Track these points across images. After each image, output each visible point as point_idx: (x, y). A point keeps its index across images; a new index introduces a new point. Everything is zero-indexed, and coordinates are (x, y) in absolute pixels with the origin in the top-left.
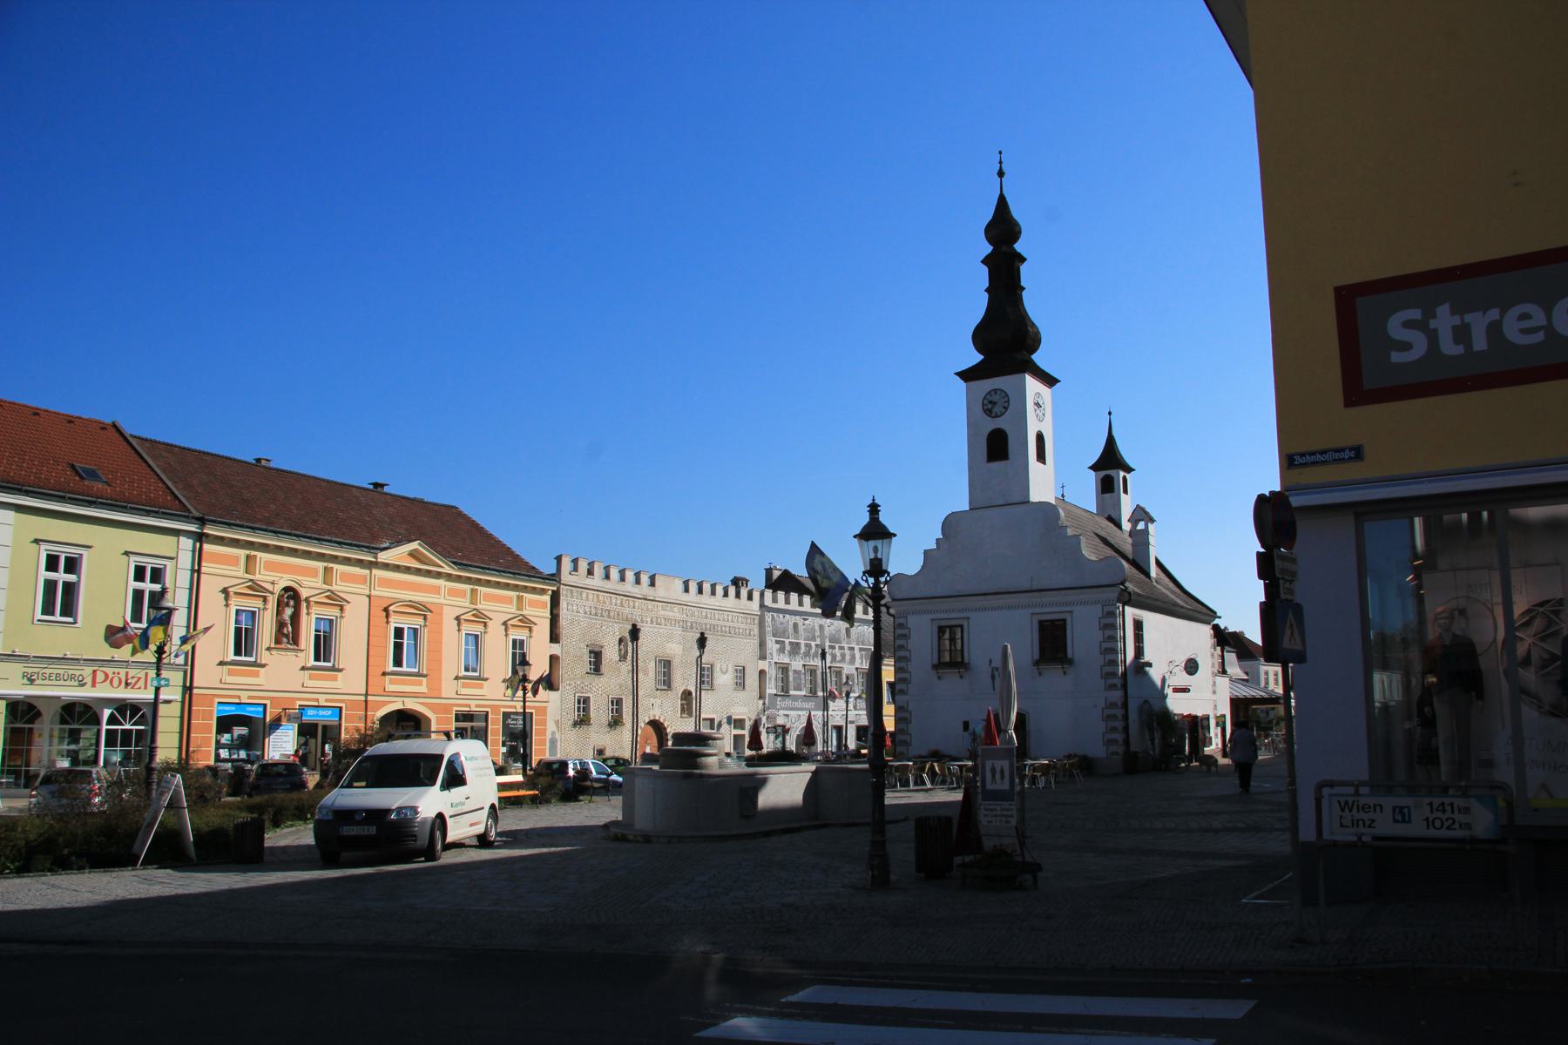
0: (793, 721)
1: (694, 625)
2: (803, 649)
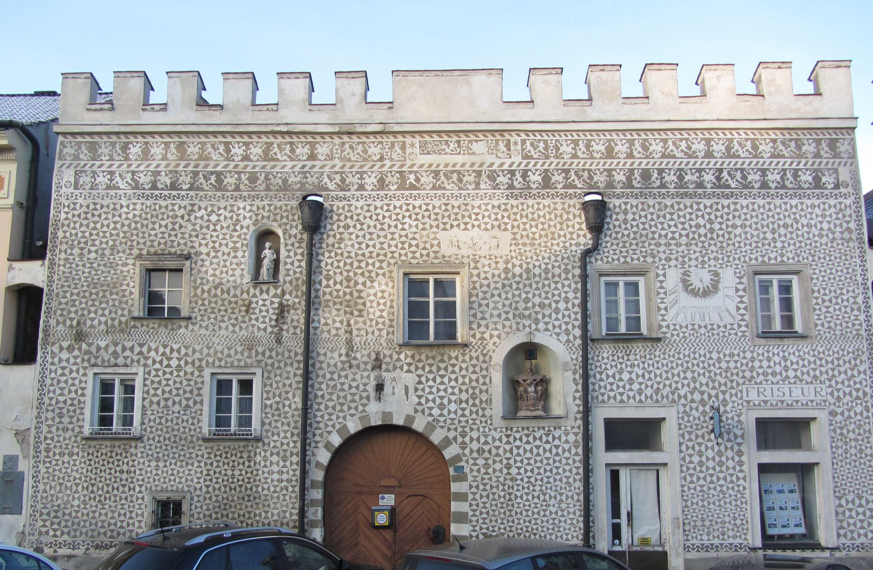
1: (557, 178)
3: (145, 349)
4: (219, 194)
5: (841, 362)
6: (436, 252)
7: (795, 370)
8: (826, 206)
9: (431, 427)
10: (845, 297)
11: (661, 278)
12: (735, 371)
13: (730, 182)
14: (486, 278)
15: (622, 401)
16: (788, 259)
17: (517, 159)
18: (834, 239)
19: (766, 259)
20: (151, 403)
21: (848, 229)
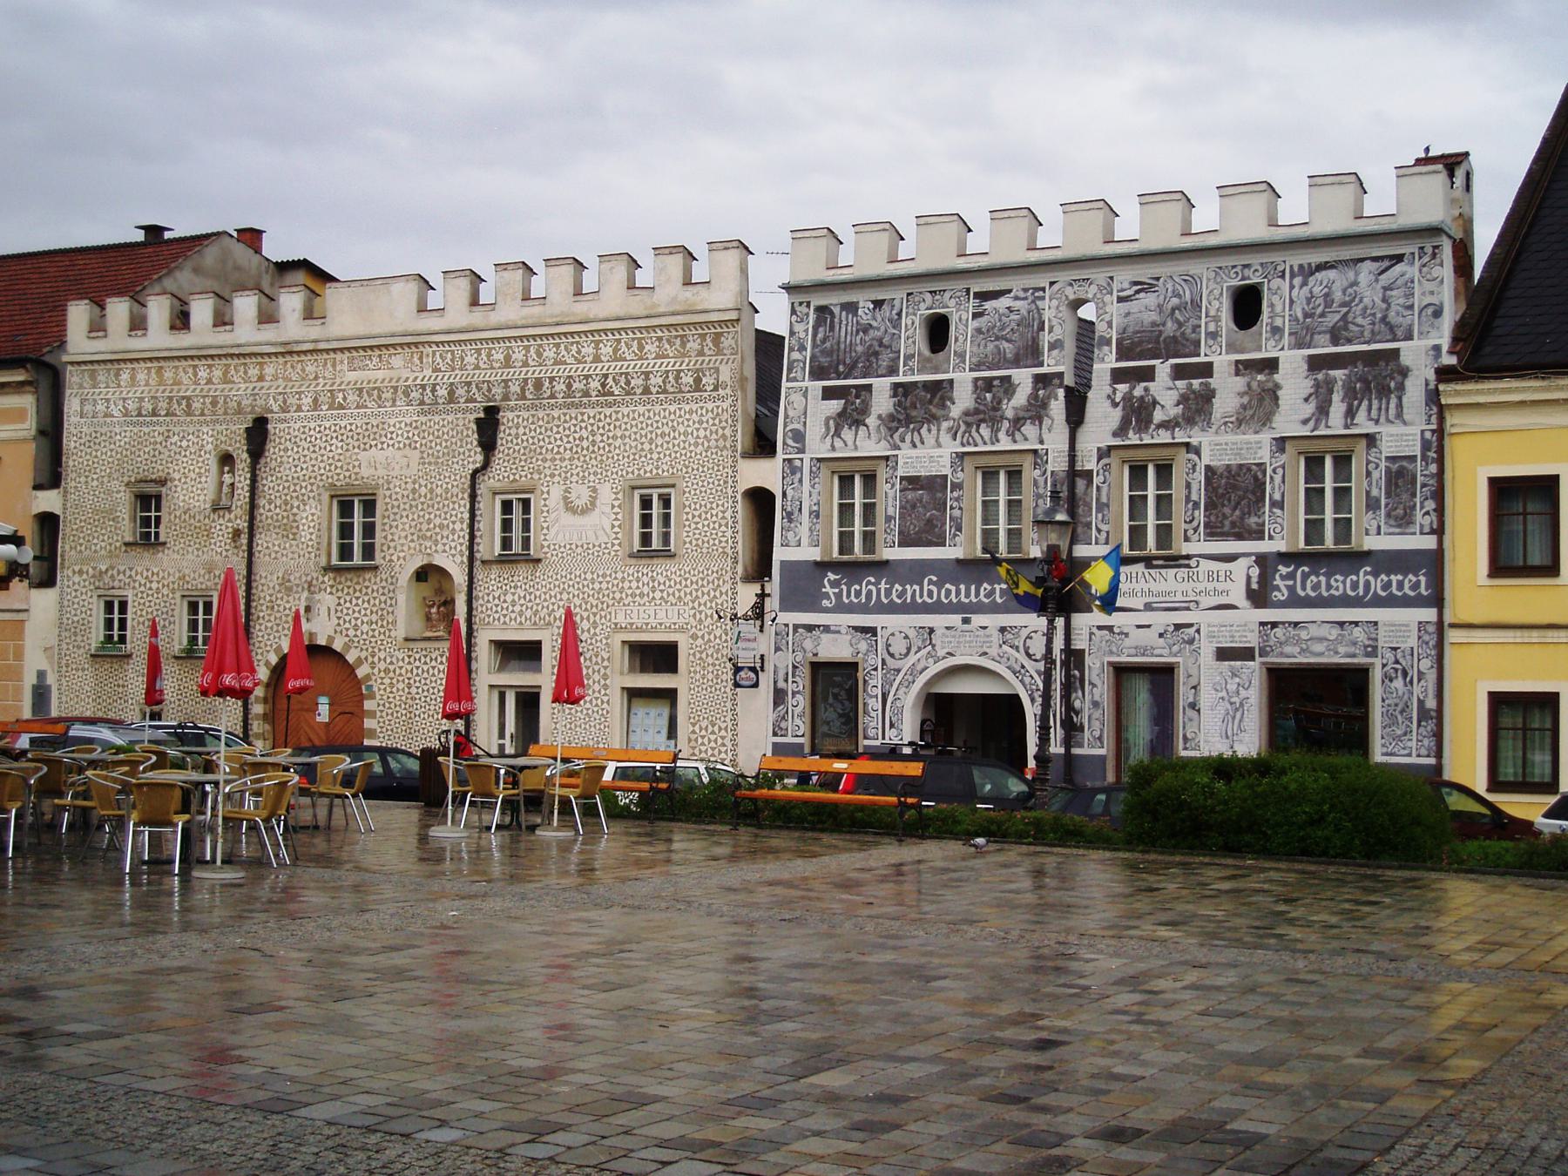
1: (461, 392)
2: (963, 399)
3: (133, 573)
4: (189, 419)
5: (705, 583)
6: (356, 474)
7: (662, 591)
8: (704, 412)
9: (347, 647)
10: (714, 512)
11: (545, 496)
12: (606, 592)
13: (614, 389)
14: (397, 499)
15: (505, 623)
17: (428, 372)
20: (139, 623)
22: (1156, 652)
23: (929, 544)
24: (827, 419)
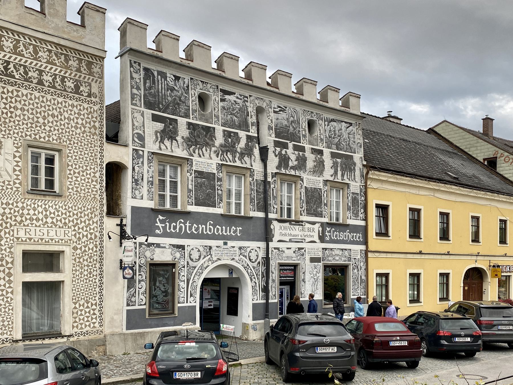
0: (195, 255)
2: (219, 139)
5: (83, 215)
7: (53, 218)
10: (88, 172)
16: (53, 140)
18: (85, 131)
19: (37, 137)
21: (94, 126)
22: (293, 259)
23: (209, 206)
24: (156, 132)
